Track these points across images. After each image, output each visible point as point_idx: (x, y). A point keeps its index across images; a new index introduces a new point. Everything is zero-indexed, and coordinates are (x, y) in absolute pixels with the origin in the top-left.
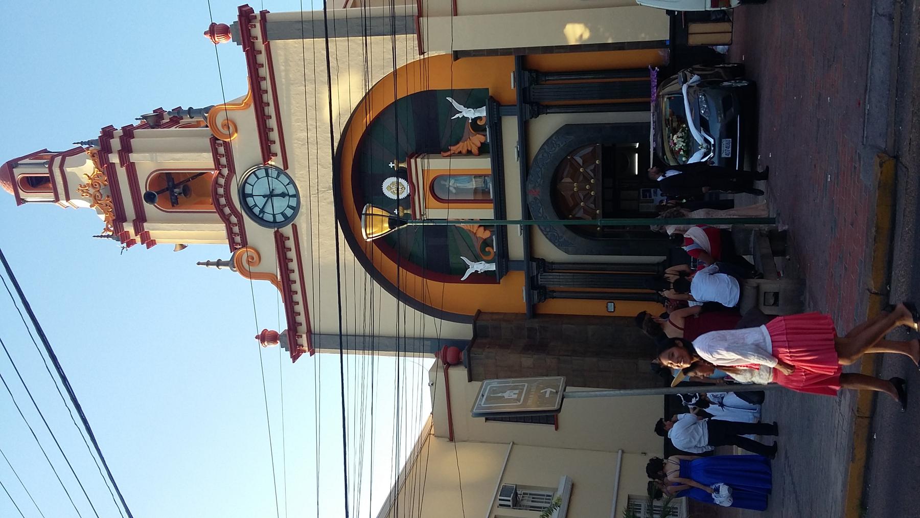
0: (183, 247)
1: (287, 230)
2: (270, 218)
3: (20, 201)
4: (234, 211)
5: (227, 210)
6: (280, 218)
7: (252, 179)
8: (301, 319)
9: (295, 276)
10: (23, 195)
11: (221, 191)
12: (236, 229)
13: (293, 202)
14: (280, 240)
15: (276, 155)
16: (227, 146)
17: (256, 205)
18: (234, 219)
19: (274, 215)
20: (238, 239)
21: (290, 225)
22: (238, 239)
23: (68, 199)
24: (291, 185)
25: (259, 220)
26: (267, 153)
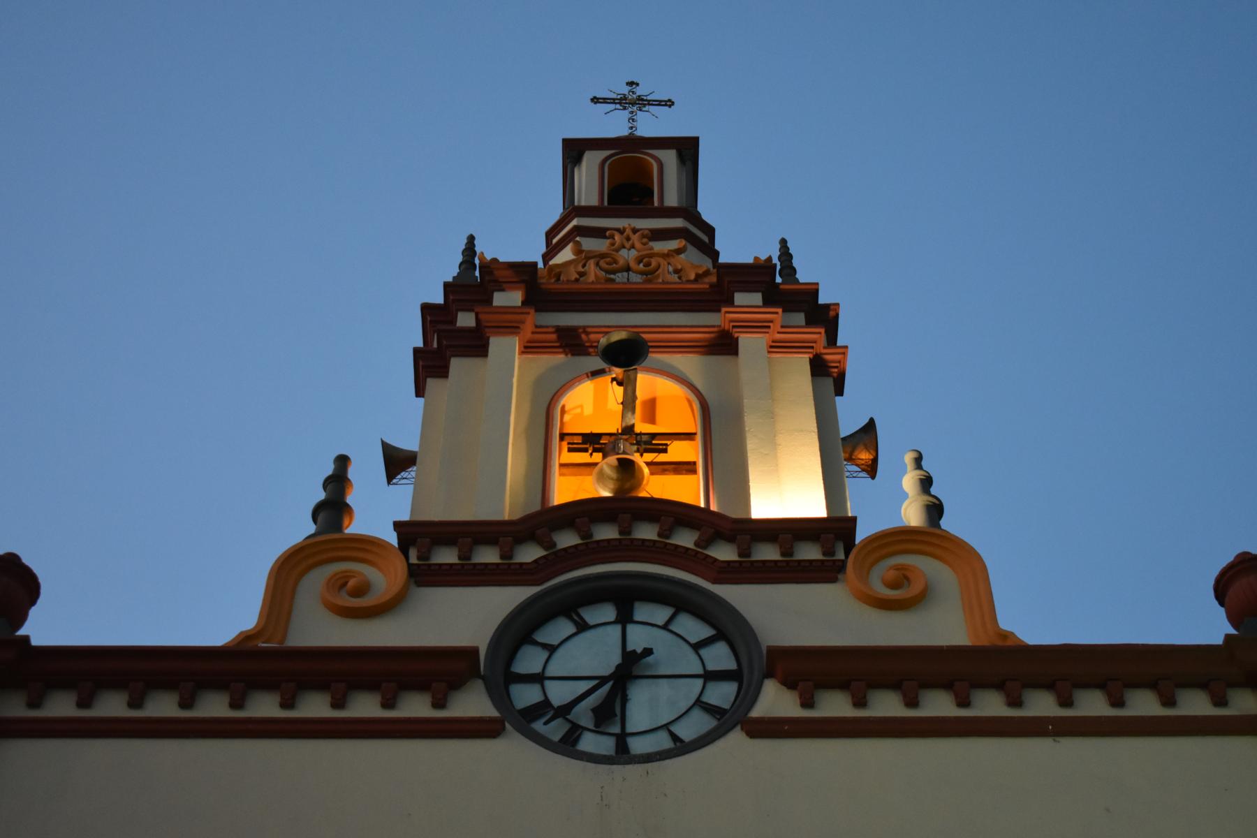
0: (397, 462)
1: (473, 703)
2: (530, 660)
3: (574, 150)
4: (558, 560)
5: (567, 540)
6: (525, 696)
7: (694, 629)
8: (61, 706)
9: (265, 706)
10: (591, 160)
11: (647, 532)
12: (488, 556)
13: (589, 742)
14: (440, 670)
15: (807, 703)
16: (827, 572)
17: (583, 627)
18: (529, 554)
19: (539, 679)
20: (447, 556)
21: (492, 712)
22: (447, 556)
23: (579, 231)
24: (667, 743)
25: (519, 631)
26: (809, 669)
